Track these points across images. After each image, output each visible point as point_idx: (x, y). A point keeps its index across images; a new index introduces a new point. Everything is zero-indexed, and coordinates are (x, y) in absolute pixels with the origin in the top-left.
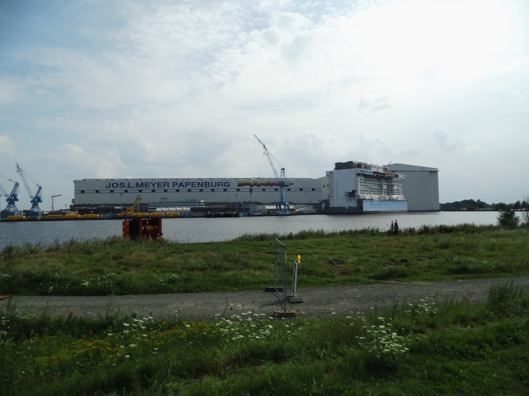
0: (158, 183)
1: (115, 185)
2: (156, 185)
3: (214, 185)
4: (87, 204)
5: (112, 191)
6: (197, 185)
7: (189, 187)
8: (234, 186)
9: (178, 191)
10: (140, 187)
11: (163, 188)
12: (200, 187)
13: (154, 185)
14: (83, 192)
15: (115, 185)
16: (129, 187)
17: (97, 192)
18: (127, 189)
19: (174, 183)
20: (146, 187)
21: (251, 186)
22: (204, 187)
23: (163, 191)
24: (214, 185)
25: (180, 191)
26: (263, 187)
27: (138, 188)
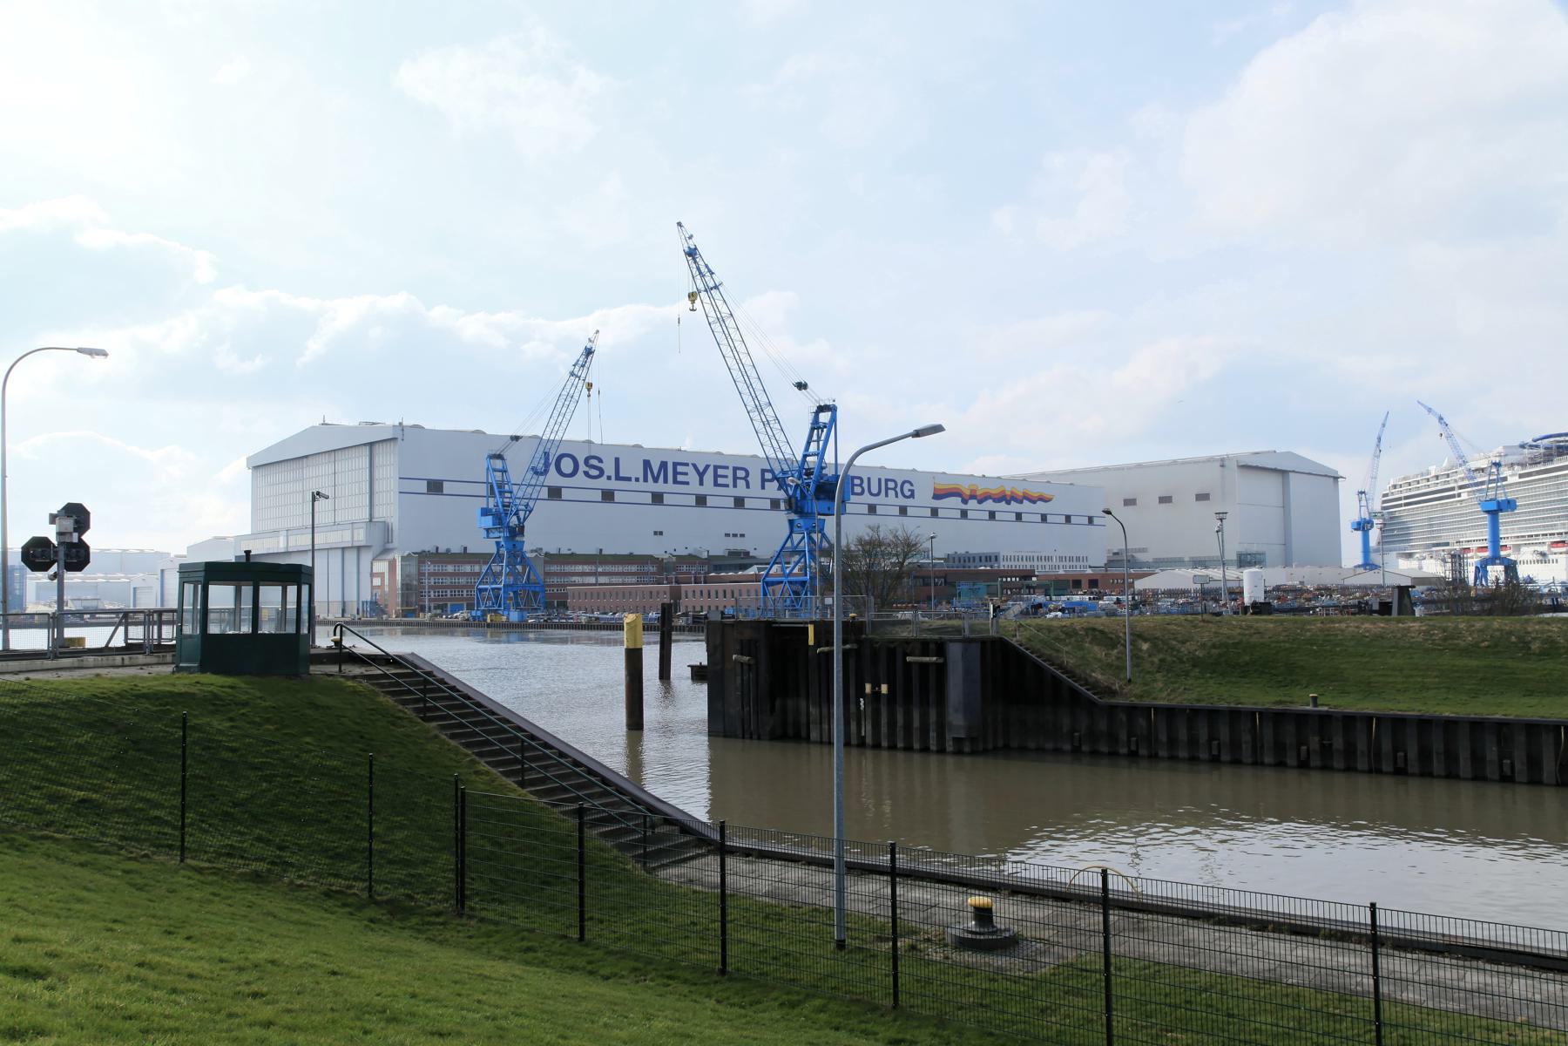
0: (716, 468)
1: (567, 465)
2: (711, 470)
3: (875, 490)
4: (456, 549)
5: (555, 493)
8: (924, 497)
10: (656, 480)
11: (731, 491)
13: (701, 475)
14: (435, 487)
15: (567, 465)
16: (618, 478)
18: (613, 484)
19: (763, 471)
20: (675, 482)
23: (731, 502)
24: (875, 490)
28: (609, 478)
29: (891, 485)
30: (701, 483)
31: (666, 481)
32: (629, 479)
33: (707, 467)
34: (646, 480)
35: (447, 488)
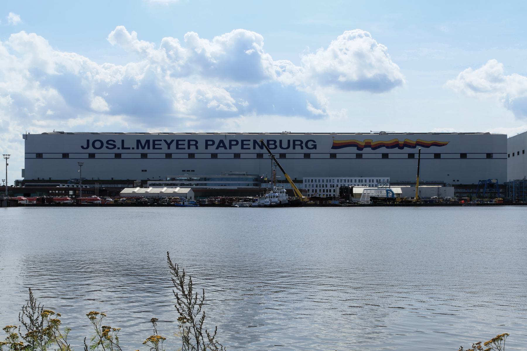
0: (177, 141)
1: (98, 144)
2: (175, 142)
3: (285, 145)
5: (92, 156)
6: (251, 146)
7: (237, 149)
8: (326, 148)
9: (214, 156)
10: (143, 148)
11: (187, 151)
12: (258, 150)
14: (39, 156)
15: (98, 144)
16: (123, 148)
17: (65, 156)
18: (121, 151)
19: (207, 141)
20: (154, 148)
21: (360, 148)
24: (285, 145)
25: (219, 156)
26: (384, 150)
27: (141, 150)
28: (119, 148)
29: (299, 143)
30: (169, 148)
31: (149, 148)
32: (129, 148)
33: (172, 141)
34: (138, 148)
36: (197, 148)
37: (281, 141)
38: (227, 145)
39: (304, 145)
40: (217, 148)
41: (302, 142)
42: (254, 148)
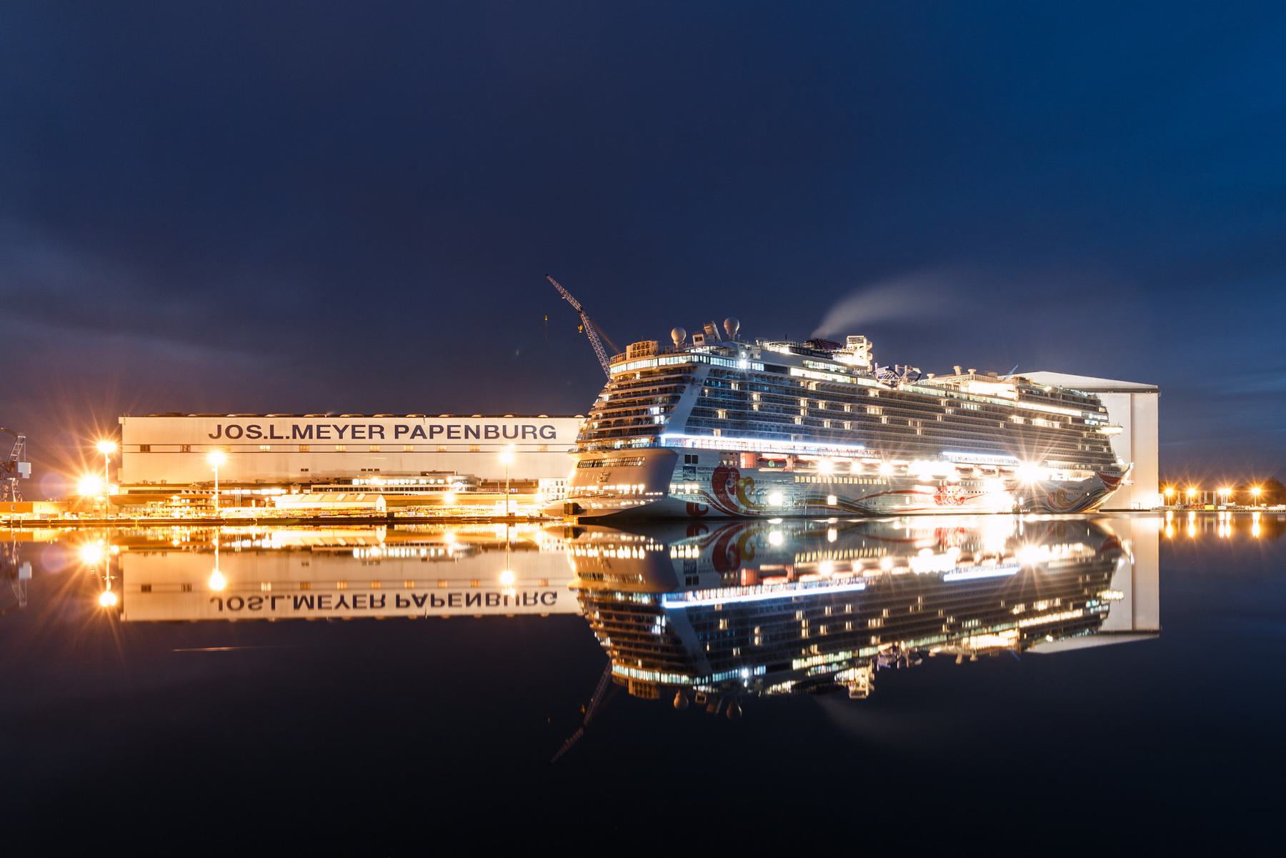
0: (354, 427)
2: (349, 429)
6: (462, 434)
10: (303, 437)
13: (341, 433)
15: (234, 432)
16: (272, 437)
19: (397, 427)
20: (319, 437)
22: (482, 439)
29: (531, 429)
30: (341, 437)
31: (311, 437)
34: (294, 437)
35: (152, 449)
36: (382, 437)
37: (504, 427)
38: (428, 434)
39: (537, 432)
40: (412, 437)
41: (535, 429)
42: (467, 437)
